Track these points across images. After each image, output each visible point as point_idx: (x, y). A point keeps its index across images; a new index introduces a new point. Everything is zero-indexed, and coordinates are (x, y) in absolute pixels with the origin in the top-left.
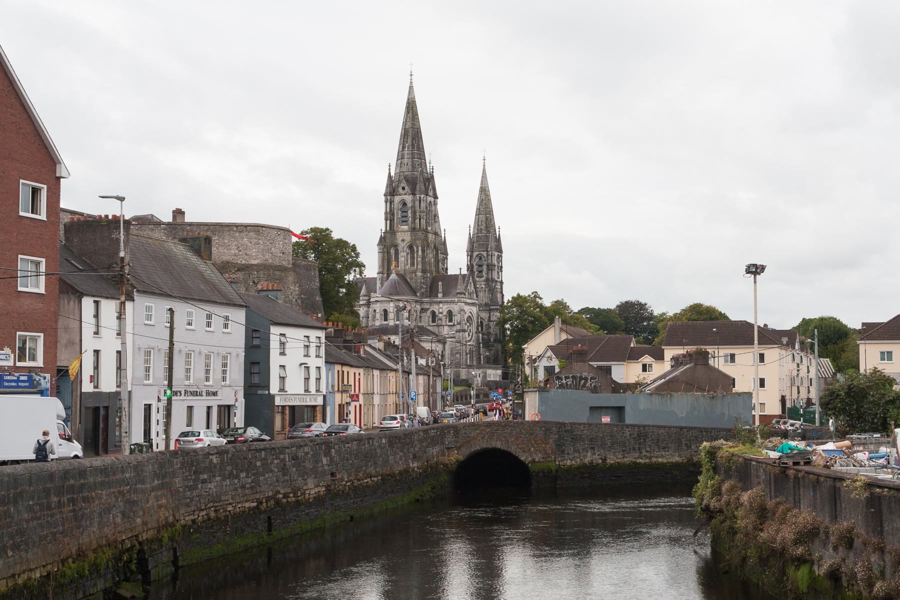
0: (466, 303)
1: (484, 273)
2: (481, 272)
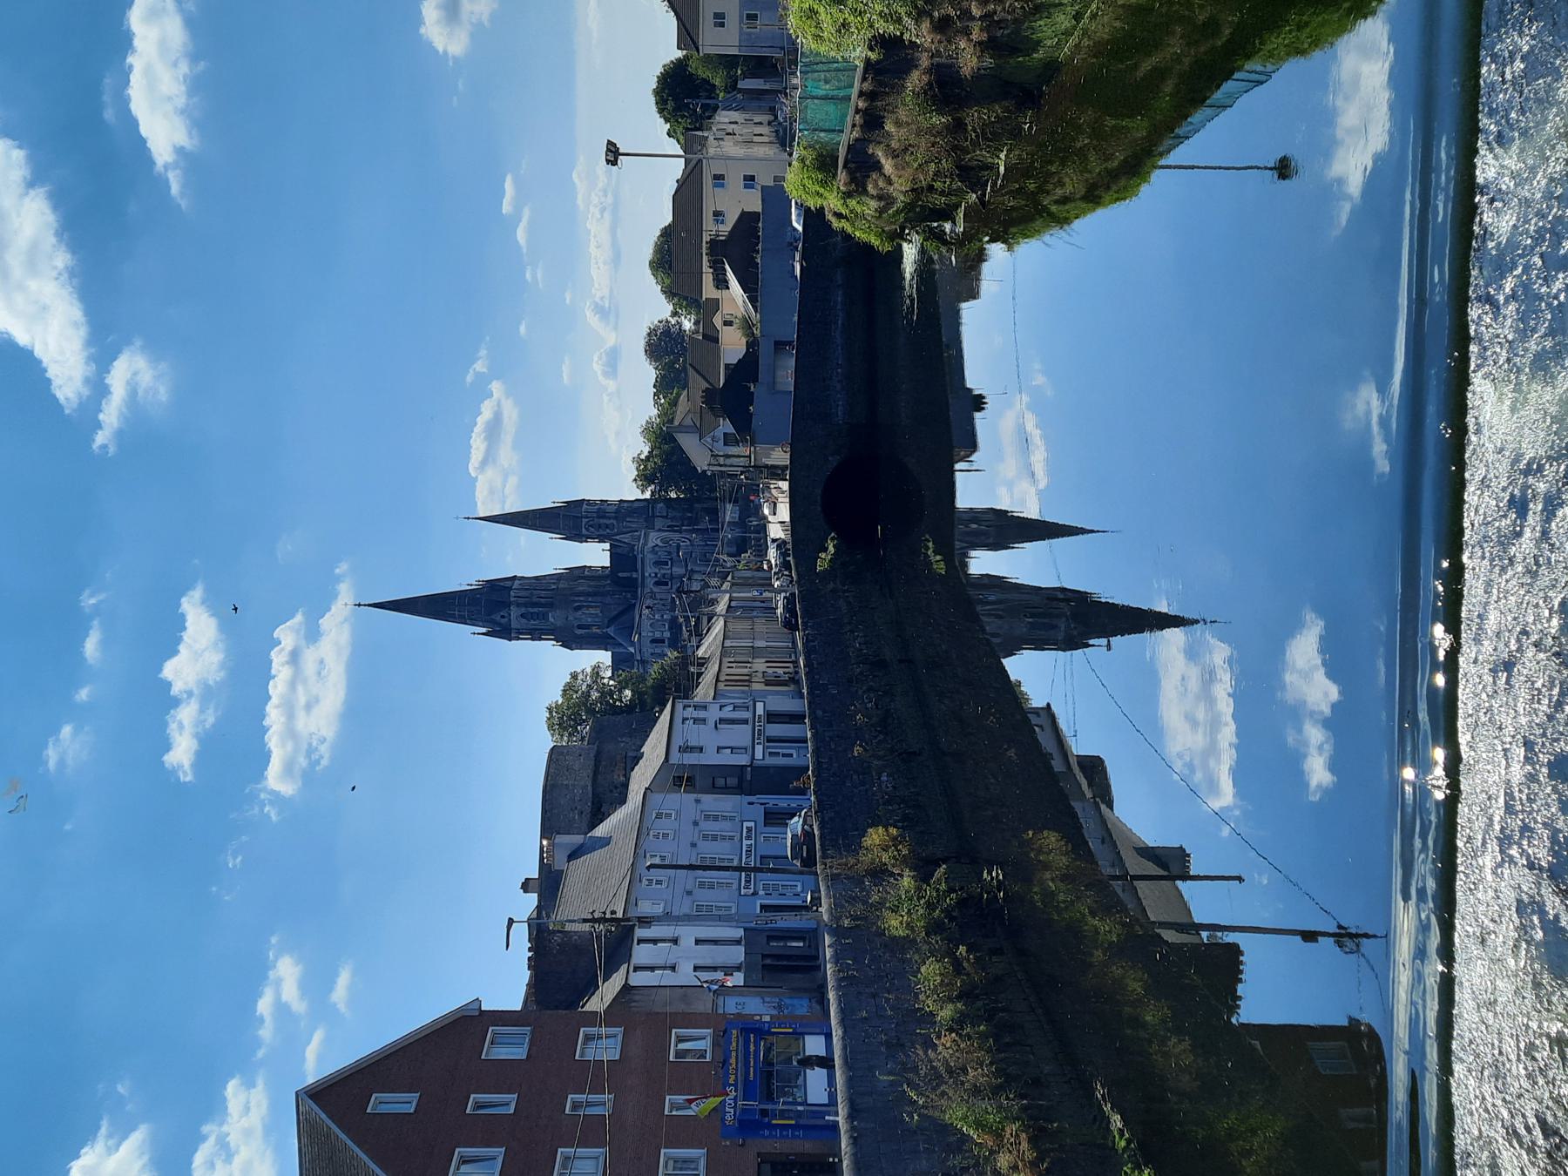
0: (645, 544)
1: (608, 522)
2: (607, 526)
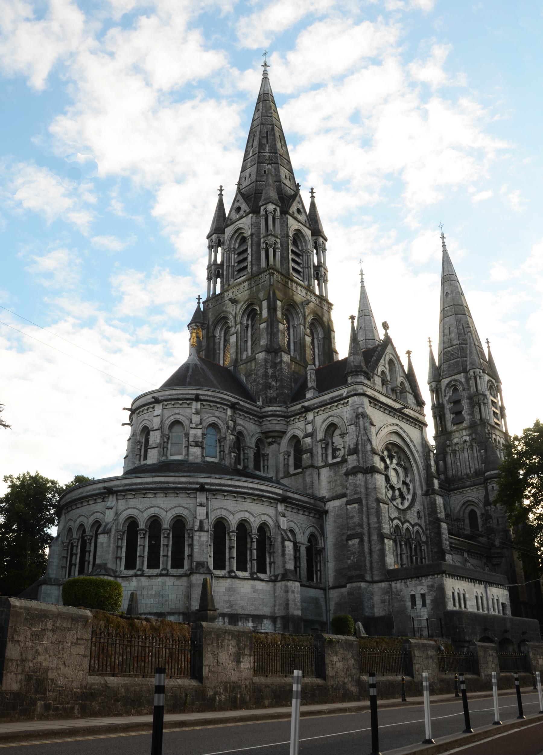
0: (374, 401)
1: (465, 414)
2: (458, 413)
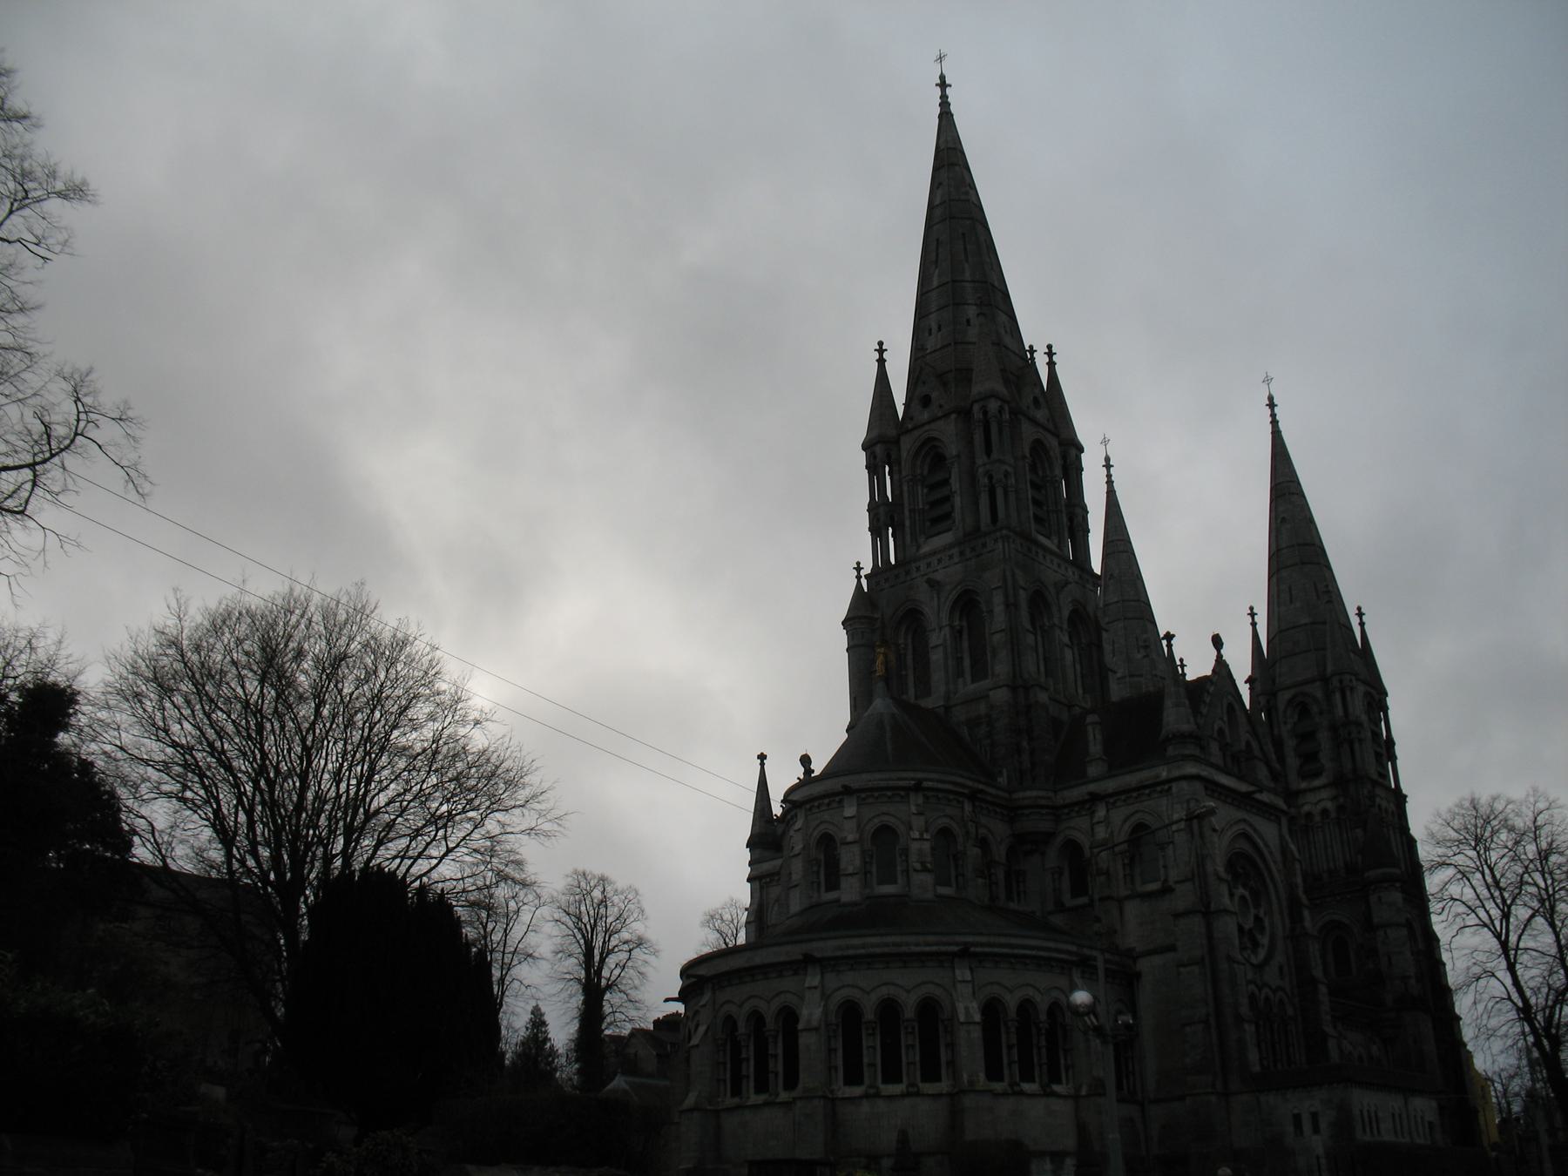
0: (1212, 787)
